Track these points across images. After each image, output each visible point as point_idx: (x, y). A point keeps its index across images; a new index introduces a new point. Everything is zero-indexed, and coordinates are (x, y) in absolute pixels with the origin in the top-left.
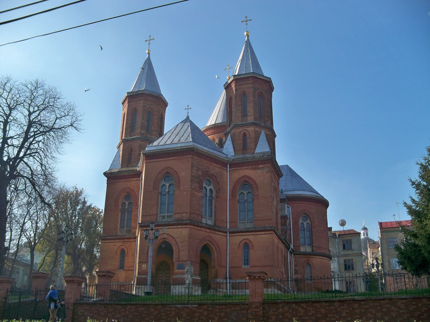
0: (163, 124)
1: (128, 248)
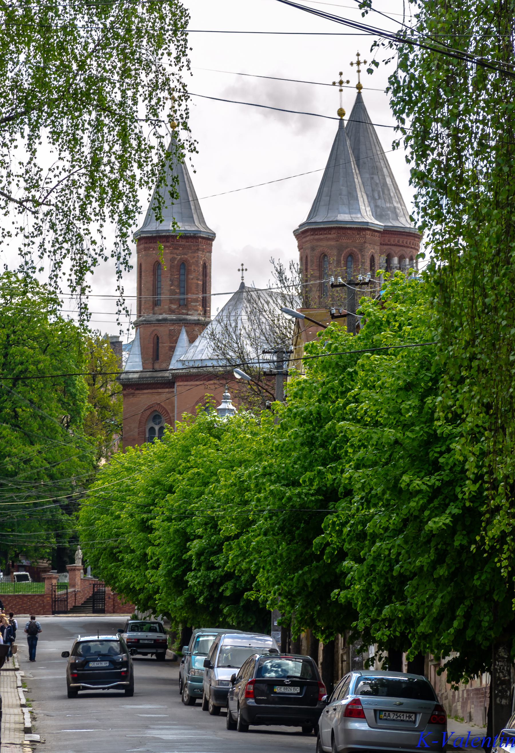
0: (208, 278)
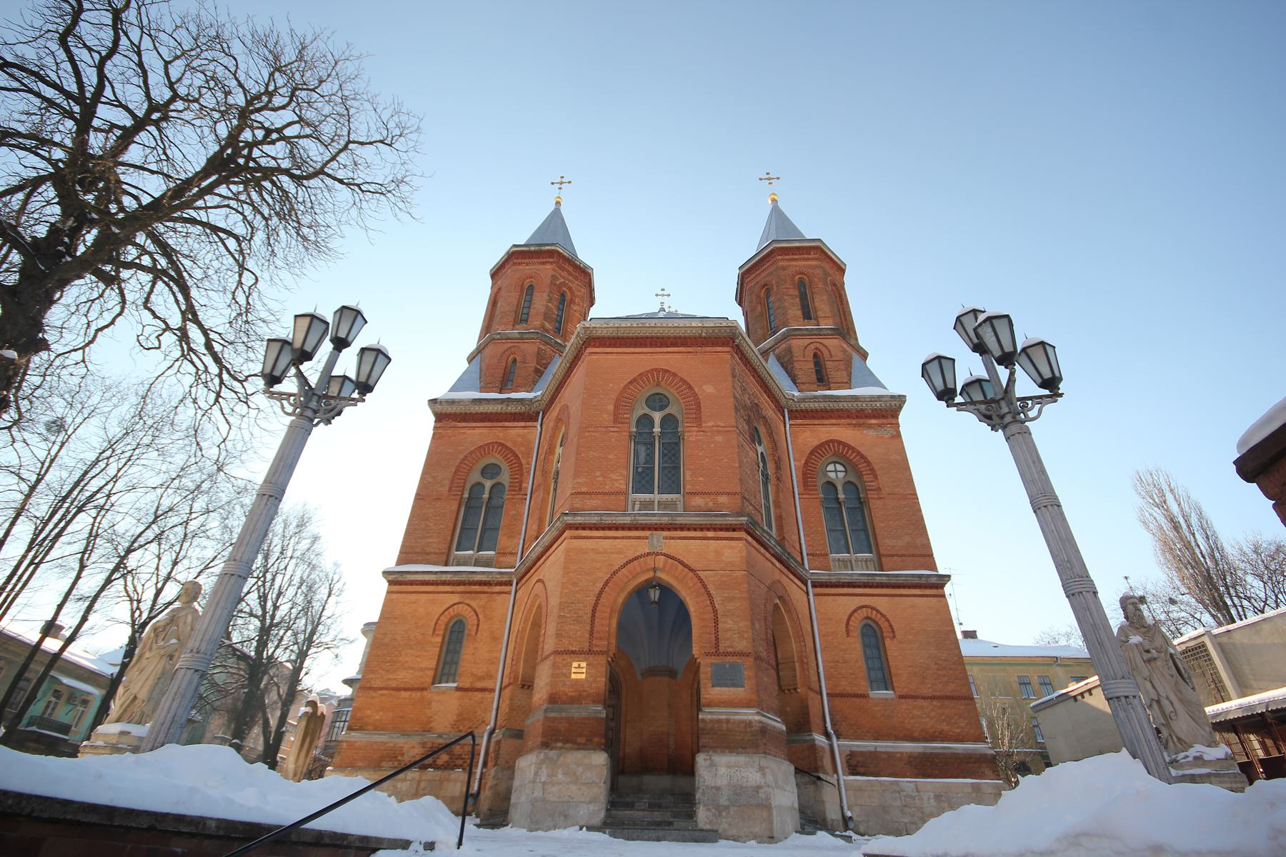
1: (479, 611)
